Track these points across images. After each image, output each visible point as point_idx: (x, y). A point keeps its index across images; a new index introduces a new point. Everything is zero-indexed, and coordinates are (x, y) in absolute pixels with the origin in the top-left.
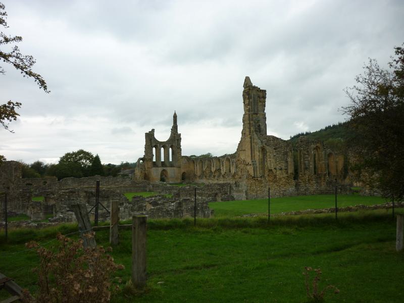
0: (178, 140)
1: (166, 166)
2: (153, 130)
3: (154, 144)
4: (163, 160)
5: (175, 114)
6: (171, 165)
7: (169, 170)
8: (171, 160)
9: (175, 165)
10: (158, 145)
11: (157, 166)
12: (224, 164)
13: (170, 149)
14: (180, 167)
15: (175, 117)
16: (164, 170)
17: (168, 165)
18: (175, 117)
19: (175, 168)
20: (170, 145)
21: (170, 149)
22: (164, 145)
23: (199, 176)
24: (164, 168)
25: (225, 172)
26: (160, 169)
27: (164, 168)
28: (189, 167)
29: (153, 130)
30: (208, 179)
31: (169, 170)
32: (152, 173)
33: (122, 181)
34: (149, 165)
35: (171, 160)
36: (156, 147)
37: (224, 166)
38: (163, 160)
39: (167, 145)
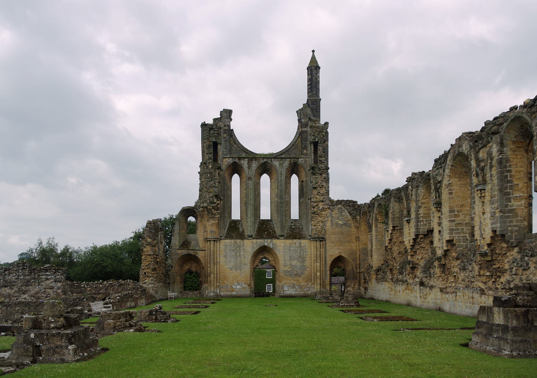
0: (316, 145)
1: (272, 236)
3: (226, 162)
4: (265, 213)
6: (295, 232)
7: (281, 247)
8: (295, 214)
9: (305, 232)
10: (245, 163)
11: (242, 236)
12: (445, 195)
13: (295, 180)
14: (322, 239)
16: (263, 250)
17: (278, 232)
19: (304, 242)
20: (287, 163)
21: (295, 180)
22: (265, 164)
23: (378, 270)
24: (267, 242)
25: (450, 242)
26: (250, 246)
27: (267, 242)
28: (358, 239)
30: (398, 281)
31: (281, 247)
32: (222, 260)
33: (27, 283)
34: (209, 229)
35: (295, 214)
36: (235, 169)
37: (445, 209)
38: (265, 213)
39: (276, 163)
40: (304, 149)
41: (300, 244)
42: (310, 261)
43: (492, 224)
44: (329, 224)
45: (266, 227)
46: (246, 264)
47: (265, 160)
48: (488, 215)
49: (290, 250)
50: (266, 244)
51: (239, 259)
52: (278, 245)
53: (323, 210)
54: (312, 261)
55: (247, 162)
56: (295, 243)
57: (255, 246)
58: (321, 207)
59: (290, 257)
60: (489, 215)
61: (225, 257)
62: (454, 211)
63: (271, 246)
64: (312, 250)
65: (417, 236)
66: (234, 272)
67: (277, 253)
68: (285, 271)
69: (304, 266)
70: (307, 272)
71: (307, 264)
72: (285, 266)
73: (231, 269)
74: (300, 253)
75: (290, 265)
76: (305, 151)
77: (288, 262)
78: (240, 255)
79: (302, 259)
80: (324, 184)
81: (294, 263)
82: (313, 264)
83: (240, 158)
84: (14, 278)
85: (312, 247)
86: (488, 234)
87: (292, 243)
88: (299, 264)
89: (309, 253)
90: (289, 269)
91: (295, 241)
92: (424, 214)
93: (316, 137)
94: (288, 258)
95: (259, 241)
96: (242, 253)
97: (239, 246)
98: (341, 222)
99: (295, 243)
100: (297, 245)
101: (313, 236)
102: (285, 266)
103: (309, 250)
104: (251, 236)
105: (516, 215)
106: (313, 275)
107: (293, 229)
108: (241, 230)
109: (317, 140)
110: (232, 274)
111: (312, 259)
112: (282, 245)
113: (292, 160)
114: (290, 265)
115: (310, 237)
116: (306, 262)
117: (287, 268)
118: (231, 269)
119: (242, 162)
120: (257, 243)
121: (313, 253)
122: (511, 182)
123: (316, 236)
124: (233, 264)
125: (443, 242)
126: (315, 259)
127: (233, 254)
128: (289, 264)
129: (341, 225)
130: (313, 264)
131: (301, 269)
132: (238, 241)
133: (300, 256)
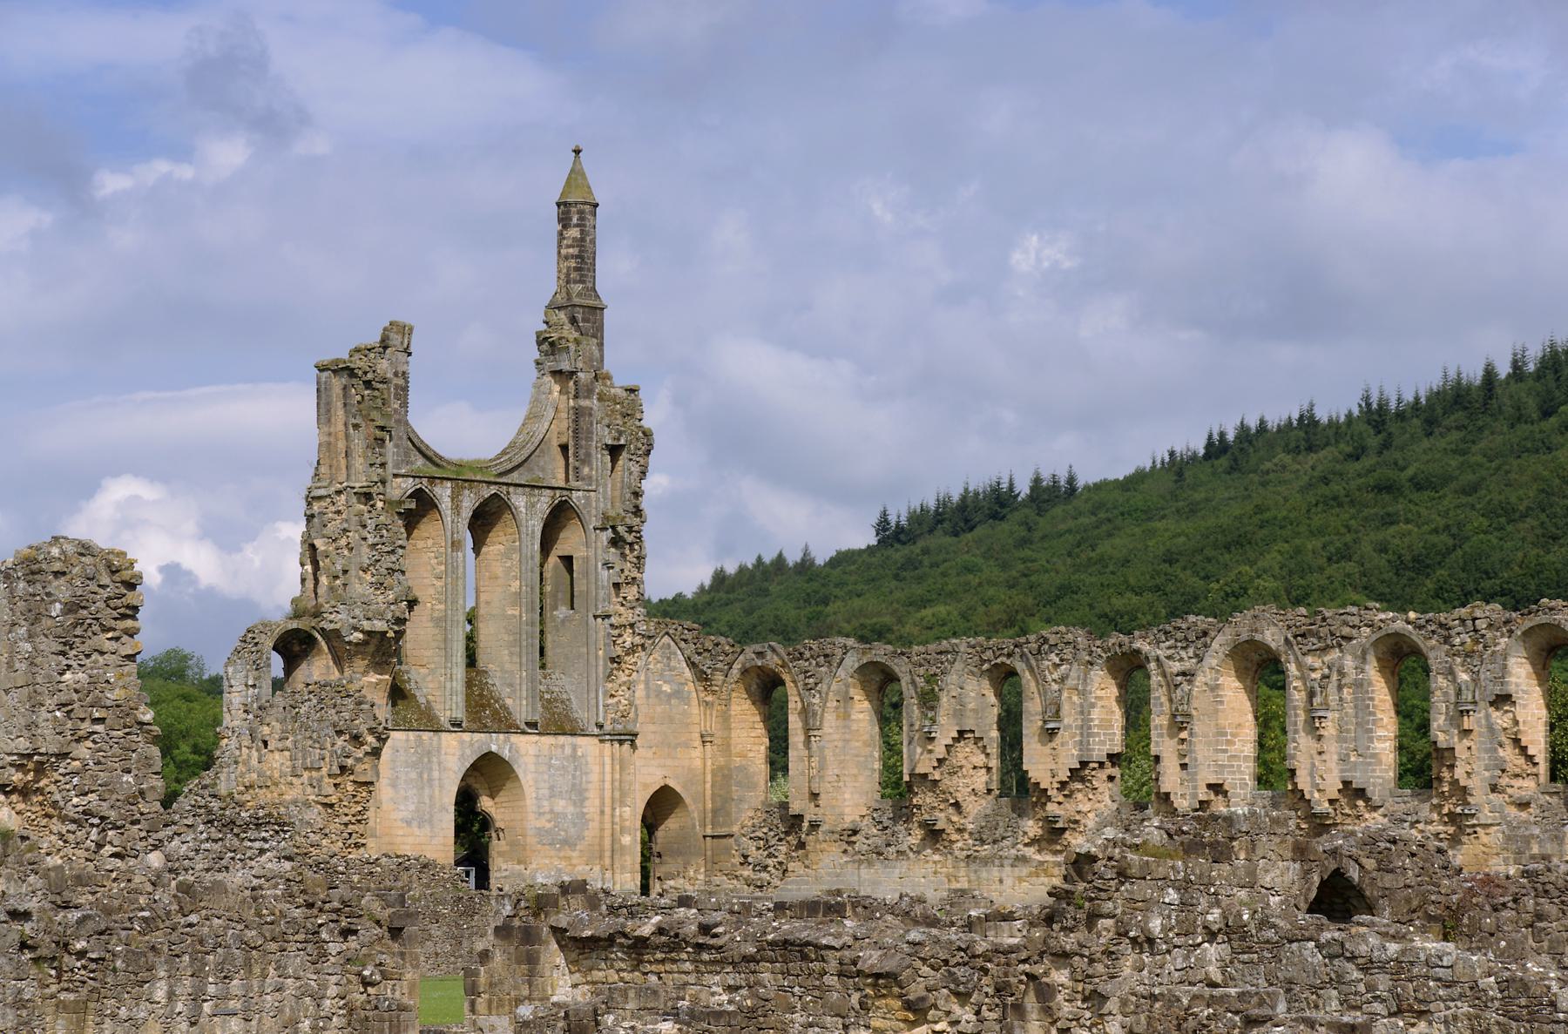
1: (505, 724)
2: (395, 339)
5: (576, 177)
9: (581, 714)
15: (575, 212)
17: (521, 708)
18: (575, 212)
24: (496, 743)
26: (455, 754)
27: (496, 743)
29: (395, 339)
40: (583, 462)
41: (574, 748)
42: (597, 802)
43: (1342, 771)
44: (640, 691)
45: (481, 695)
46: (444, 809)
47: (493, 490)
48: (1332, 758)
49: (550, 766)
50: (494, 748)
51: (427, 791)
52: (523, 752)
53: (632, 650)
54: (608, 801)
55: (449, 492)
56: (563, 746)
57: (468, 752)
58: (627, 645)
59: (552, 788)
60: (1335, 757)
61: (394, 786)
62: (1225, 734)
63: (506, 754)
64: (608, 768)
65: (1084, 764)
66: (417, 831)
67: (521, 776)
68: (540, 832)
69: (584, 814)
70: (591, 833)
71: (592, 807)
72: (540, 814)
73: (409, 823)
74: (574, 777)
75: (551, 811)
76: (586, 470)
77: (546, 803)
78: (430, 780)
79: (578, 794)
80: (635, 574)
81: (561, 805)
82: (608, 810)
83: (432, 479)
84: (185, 847)
85: (608, 760)
86: (1333, 785)
87: (556, 746)
88: (571, 809)
89: (594, 777)
90: (548, 825)
91: (562, 739)
92: (1102, 720)
93: (620, 433)
94: (546, 792)
95: (477, 736)
96: (436, 774)
97: (429, 752)
98: (666, 688)
99: (563, 746)
100: (568, 751)
101: (608, 728)
102: (540, 814)
103: (596, 769)
104: (456, 724)
105: (1380, 763)
106: (607, 842)
107: (549, 701)
108: (422, 700)
109: (622, 442)
110: (410, 840)
111: (608, 794)
112: (532, 750)
113: (558, 493)
114: (551, 811)
115: (596, 731)
116: (587, 803)
117: (544, 823)
118: (409, 823)
119: (438, 490)
120: (472, 745)
121: (608, 777)
122: (1373, 714)
123: (619, 727)
124: (412, 807)
125: (1195, 788)
126: (617, 794)
127: (413, 775)
128: (547, 809)
129: (670, 696)
130: (608, 810)
131: (575, 825)
132: (426, 736)
133: (574, 785)
